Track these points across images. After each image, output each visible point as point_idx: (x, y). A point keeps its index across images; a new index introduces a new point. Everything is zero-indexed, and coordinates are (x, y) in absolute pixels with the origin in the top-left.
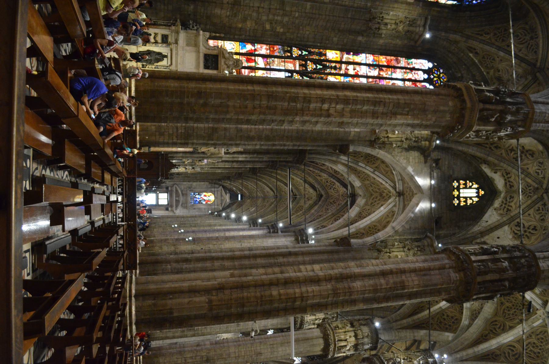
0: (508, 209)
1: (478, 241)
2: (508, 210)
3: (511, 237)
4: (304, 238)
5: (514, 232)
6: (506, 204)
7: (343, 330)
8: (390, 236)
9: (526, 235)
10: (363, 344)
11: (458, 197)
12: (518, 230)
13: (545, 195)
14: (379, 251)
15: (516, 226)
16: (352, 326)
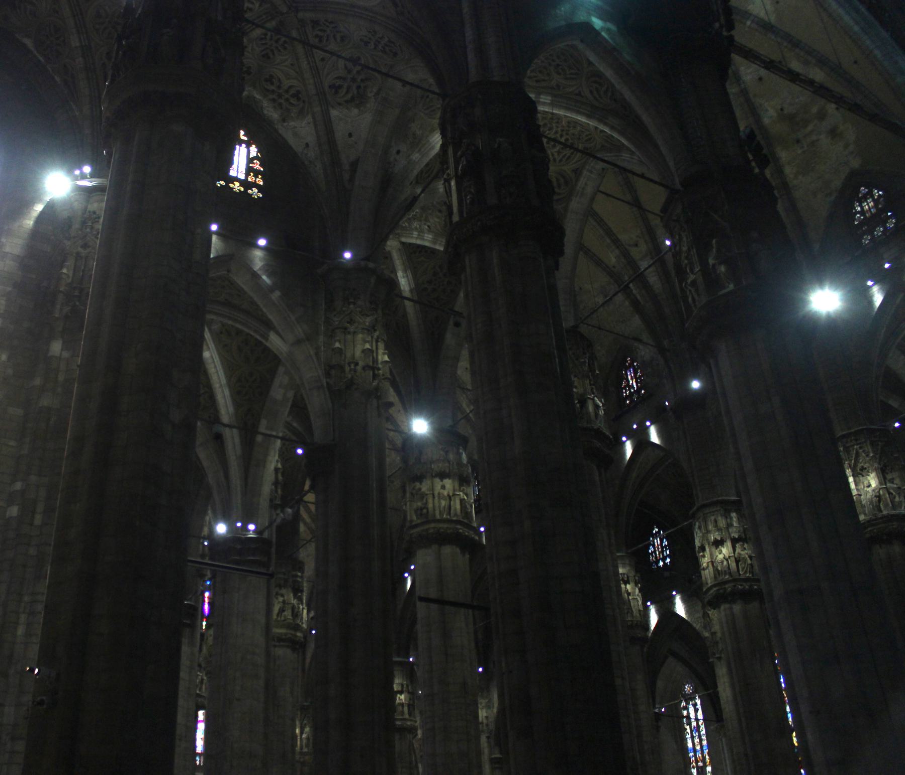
0: (293, 96)
1: (346, 176)
2: (297, 95)
3: (356, 111)
4: (239, 547)
5: (347, 102)
6: (280, 96)
7: (430, 501)
8: (317, 354)
9: (362, 80)
10: (460, 464)
11: (245, 183)
12: (347, 92)
13: (301, 15)
14: (351, 384)
15: (336, 92)
16: (420, 478)
